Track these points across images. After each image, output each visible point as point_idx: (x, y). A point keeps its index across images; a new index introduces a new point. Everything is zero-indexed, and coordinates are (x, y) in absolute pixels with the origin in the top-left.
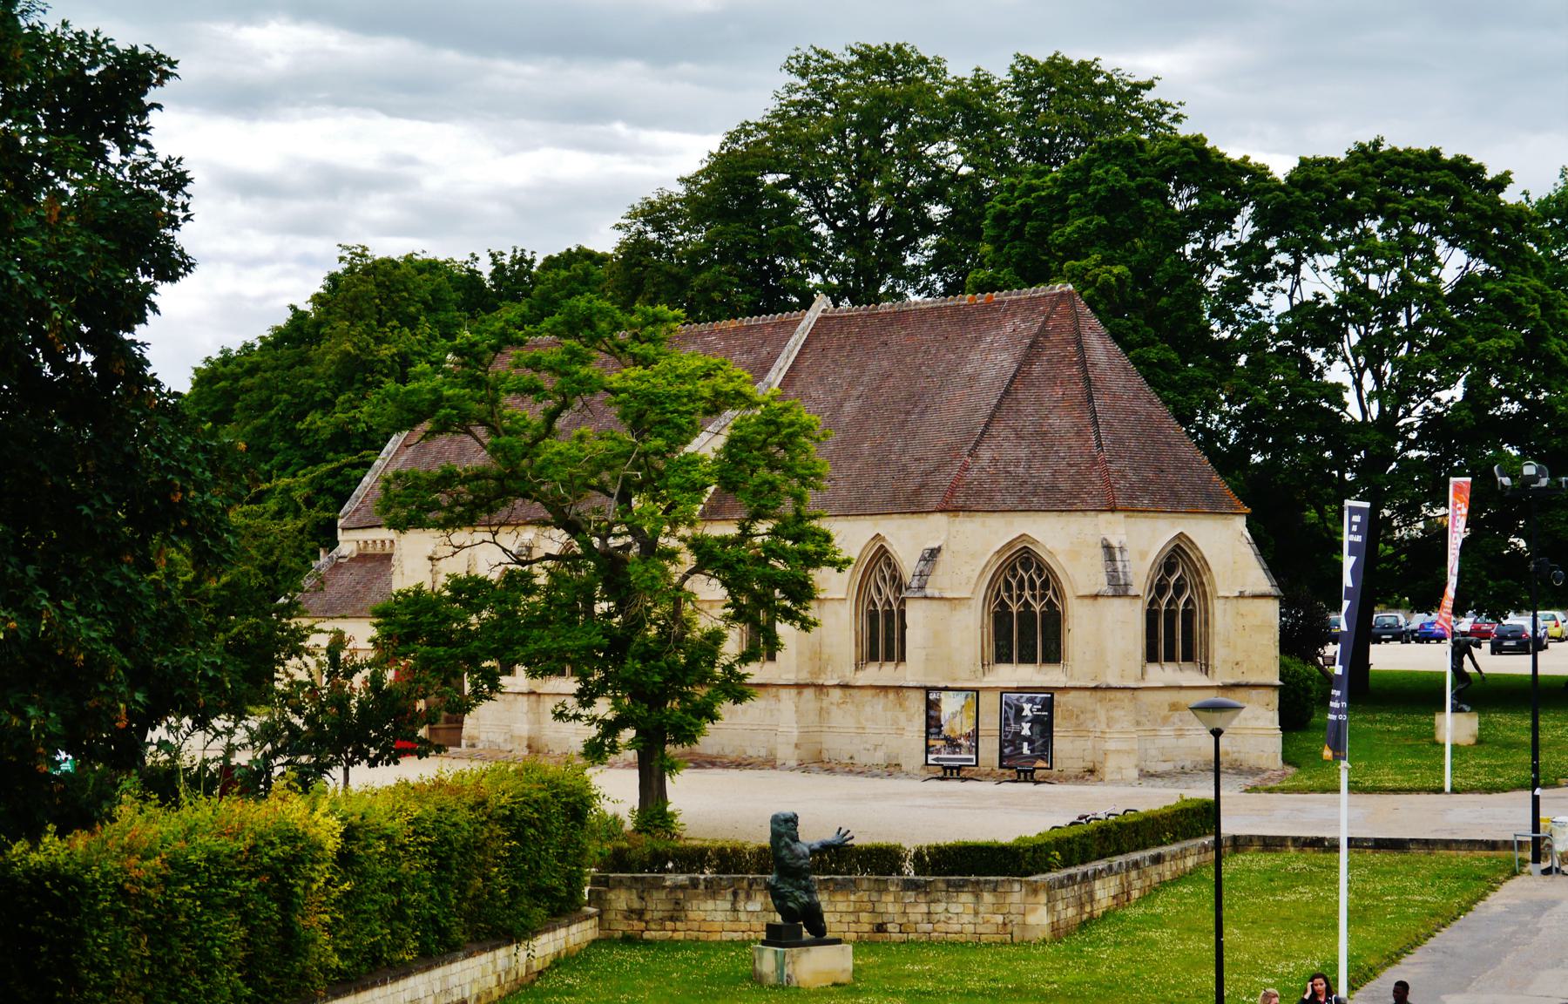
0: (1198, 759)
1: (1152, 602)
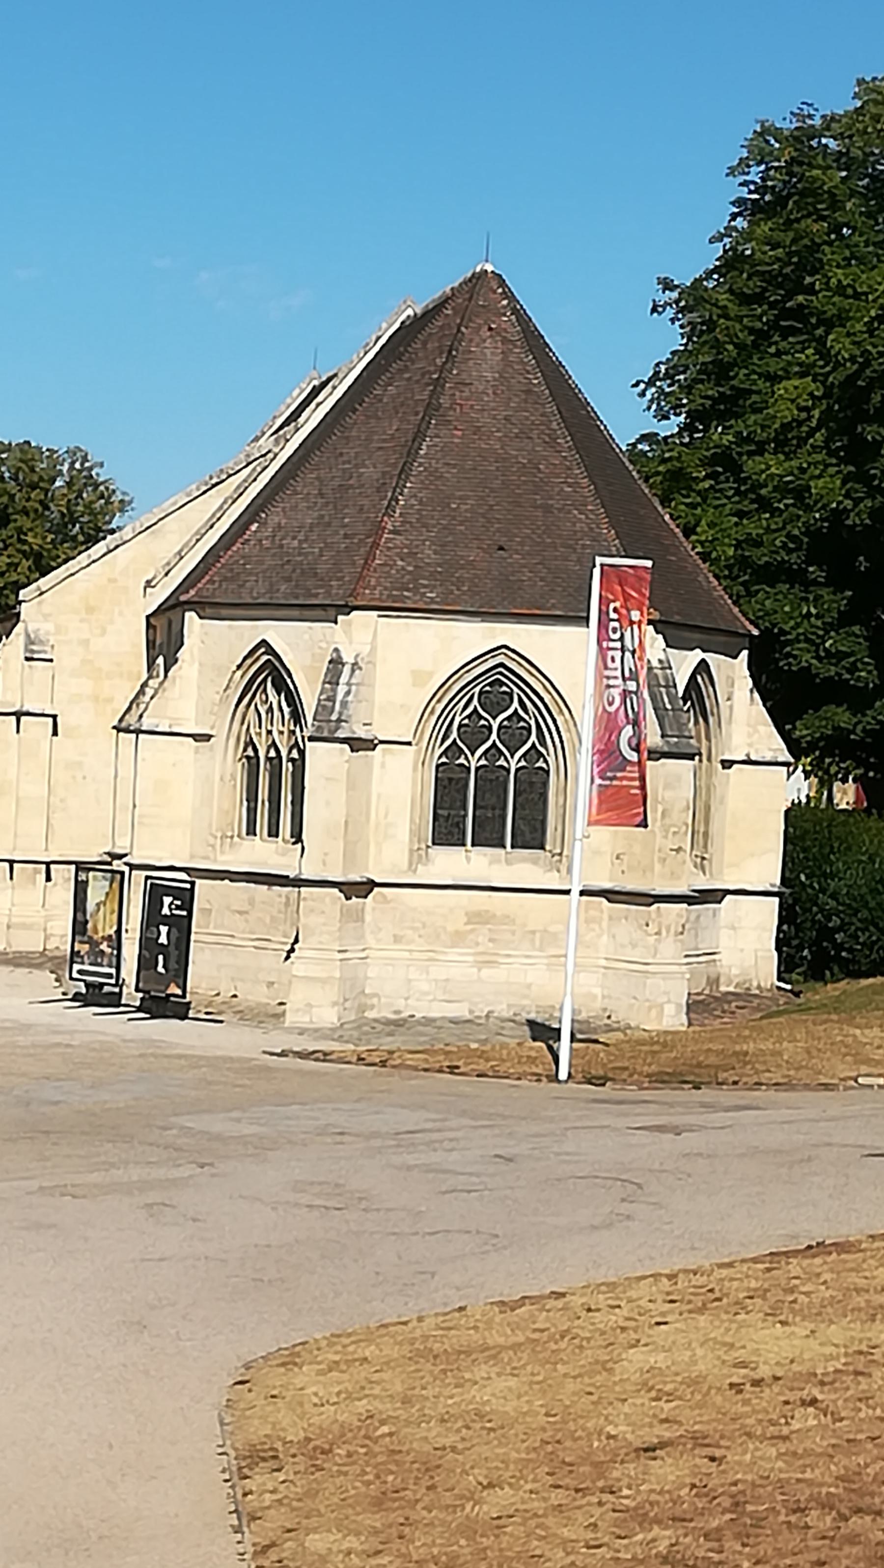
0: (526, 1002)
1: (453, 751)
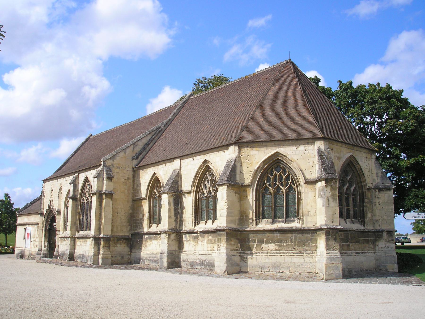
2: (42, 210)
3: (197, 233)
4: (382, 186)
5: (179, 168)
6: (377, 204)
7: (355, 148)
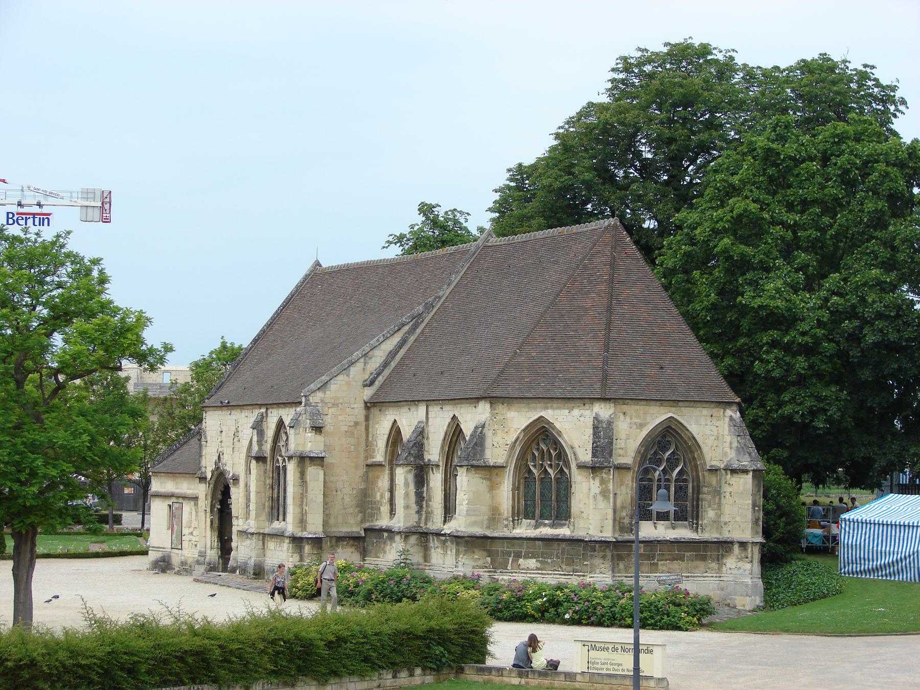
1: (646, 471)
2: (203, 469)
3: (444, 535)
4: (735, 466)
5: (425, 420)
6: (728, 495)
7: (680, 404)
